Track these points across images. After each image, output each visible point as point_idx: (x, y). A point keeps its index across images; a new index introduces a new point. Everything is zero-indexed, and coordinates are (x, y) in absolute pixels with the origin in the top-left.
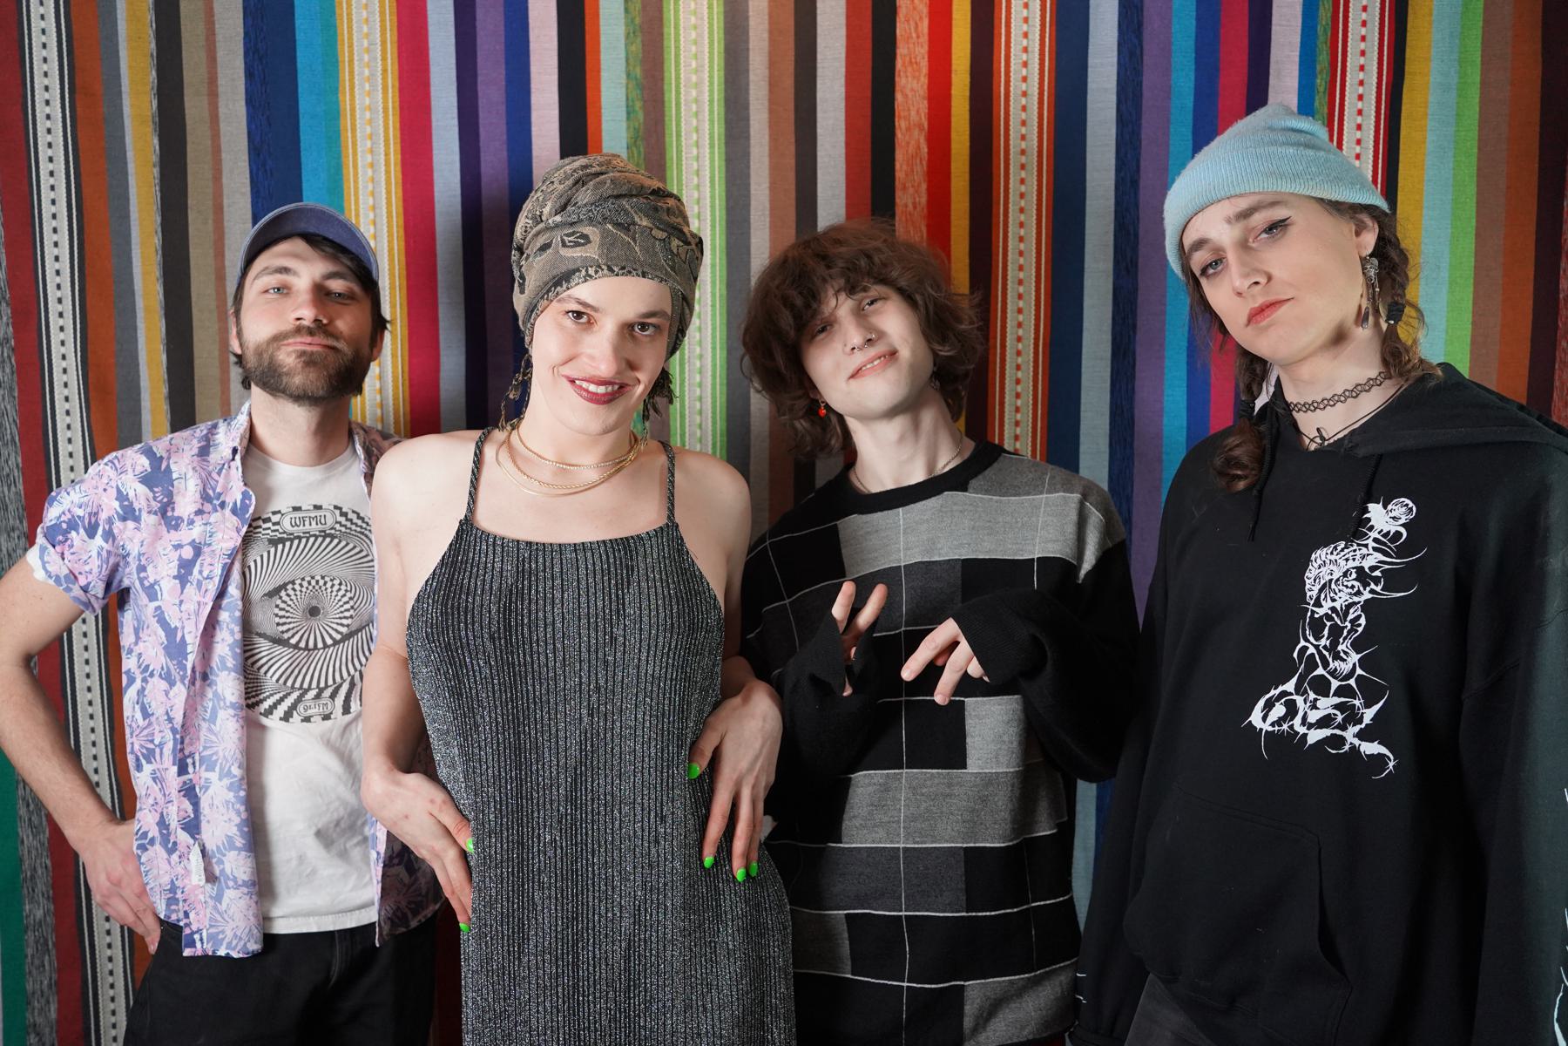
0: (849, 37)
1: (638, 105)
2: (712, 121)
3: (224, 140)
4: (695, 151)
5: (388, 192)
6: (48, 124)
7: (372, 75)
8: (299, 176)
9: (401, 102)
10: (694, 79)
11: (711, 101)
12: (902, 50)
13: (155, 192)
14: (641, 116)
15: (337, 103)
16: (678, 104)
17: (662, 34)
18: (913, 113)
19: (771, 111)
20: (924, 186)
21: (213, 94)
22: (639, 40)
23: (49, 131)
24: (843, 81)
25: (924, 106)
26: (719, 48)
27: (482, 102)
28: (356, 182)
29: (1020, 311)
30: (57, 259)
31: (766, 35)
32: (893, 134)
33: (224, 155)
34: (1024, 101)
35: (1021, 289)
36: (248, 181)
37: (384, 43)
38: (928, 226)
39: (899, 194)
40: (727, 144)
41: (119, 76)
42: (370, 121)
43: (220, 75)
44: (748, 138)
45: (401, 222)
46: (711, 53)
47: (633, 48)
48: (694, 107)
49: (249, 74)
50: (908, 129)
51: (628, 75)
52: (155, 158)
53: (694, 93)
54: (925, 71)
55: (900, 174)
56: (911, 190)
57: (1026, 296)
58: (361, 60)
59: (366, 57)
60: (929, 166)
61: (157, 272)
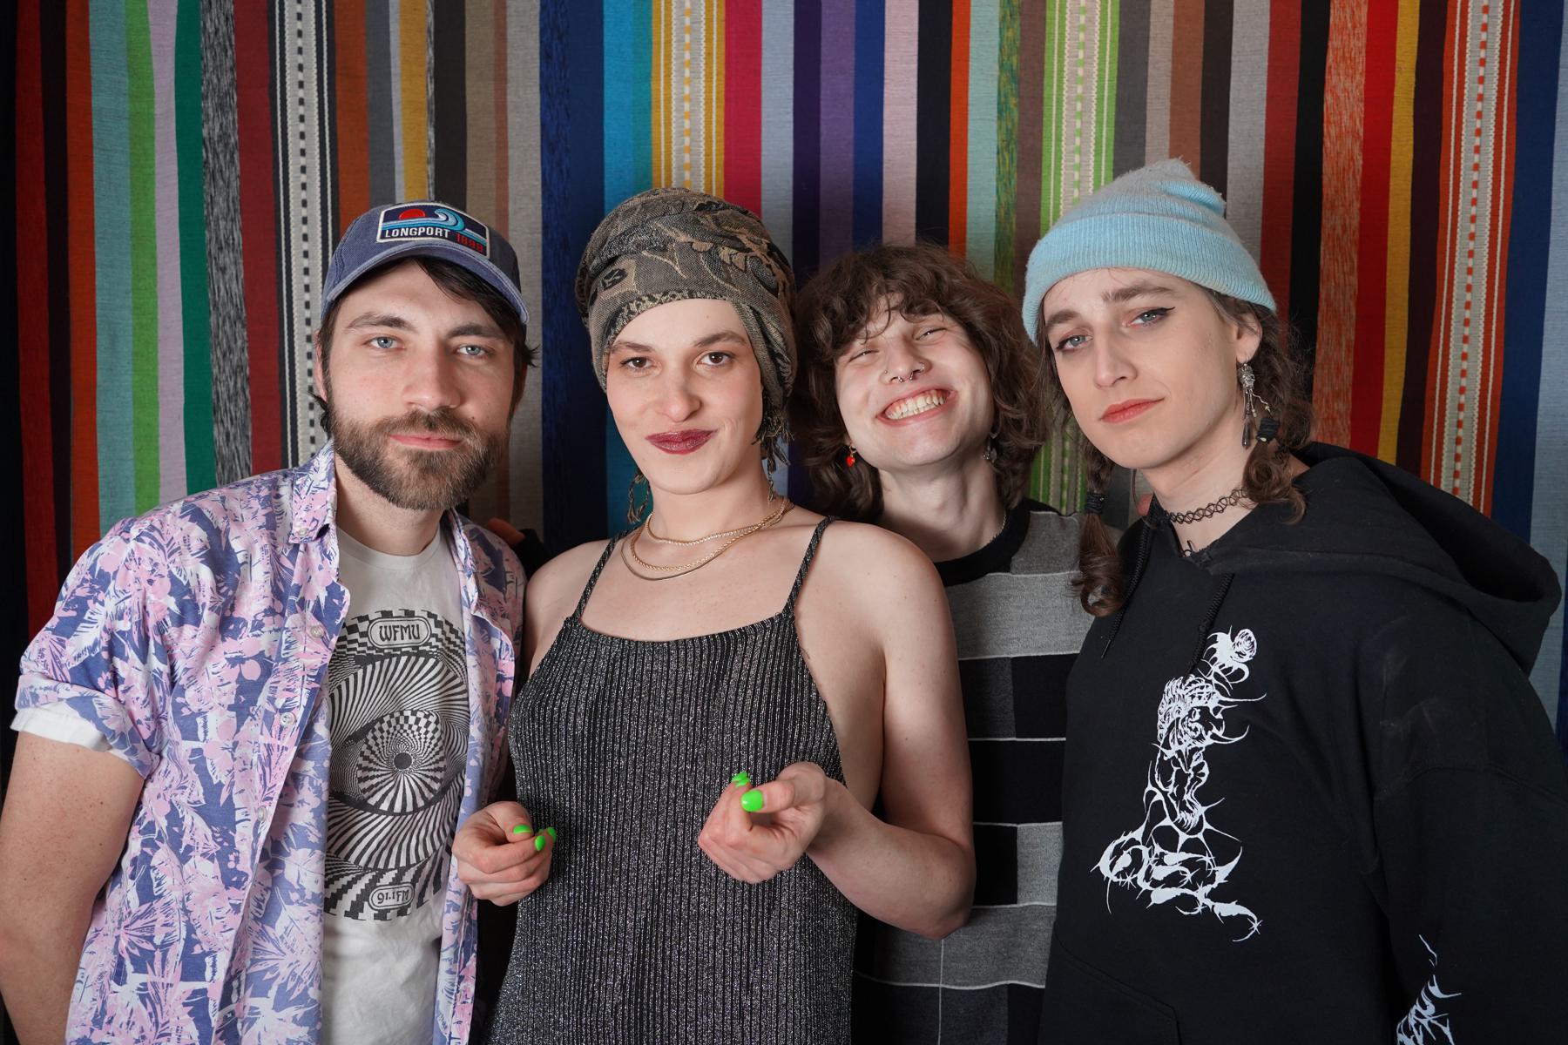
0: (1272, 24)
1: (1013, 101)
2: (1099, 123)
3: (511, 134)
4: (1077, 158)
6: (301, 110)
7: (694, 59)
9: (727, 91)
10: (1080, 72)
11: (1100, 99)
12: (1334, 42)
14: (1016, 114)
15: (648, 92)
16: (1059, 102)
17: (1043, 18)
18: (1345, 118)
19: (1173, 112)
20: (1357, 205)
21: (501, 79)
22: (1017, 25)
23: (302, 119)
24: (1264, 77)
25: (1359, 109)
26: (1112, 35)
27: (825, 93)
29: (1464, 357)
30: (306, 271)
31: (1171, 21)
32: (1321, 143)
34: (1479, 106)
35: (1467, 331)
36: (539, 183)
37: (709, 21)
38: (1361, 254)
39: (1326, 213)
41: (387, 56)
42: (689, 115)
43: (509, 57)
44: (1143, 145)
46: (1102, 41)
47: (1010, 34)
48: (1079, 105)
49: (546, 55)
50: (1339, 136)
51: (1001, 66)
53: (1080, 89)
54: (1361, 67)
55: (1328, 191)
56: (1341, 210)
57: (1472, 339)
58: (681, 40)
59: (687, 38)
60: (1363, 182)
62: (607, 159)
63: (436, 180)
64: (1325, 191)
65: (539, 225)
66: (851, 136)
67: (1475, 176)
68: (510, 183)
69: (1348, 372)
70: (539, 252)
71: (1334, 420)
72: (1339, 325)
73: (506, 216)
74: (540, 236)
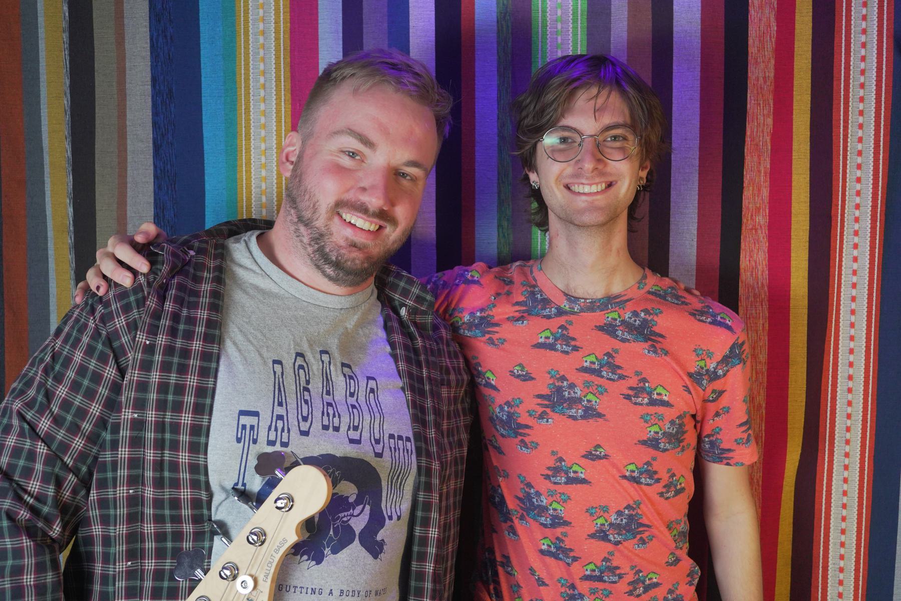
5: (277, 58)
8: (198, 45)
13: (64, 56)
28: (247, 48)
33: (126, 21)
36: (148, 46)
40: (589, 20)
44: (609, 14)
45: (289, 86)
52: (65, 24)
60: (776, 43)
61: (64, 130)
62: (202, 29)
63: (70, 45)
64: (750, 50)
65: (149, 78)
66: (386, 10)
67: (863, 38)
68: (127, 46)
69: (765, 193)
70: (150, 100)
71: (756, 230)
72: (759, 156)
73: (124, 71)
74: (150, 87)
